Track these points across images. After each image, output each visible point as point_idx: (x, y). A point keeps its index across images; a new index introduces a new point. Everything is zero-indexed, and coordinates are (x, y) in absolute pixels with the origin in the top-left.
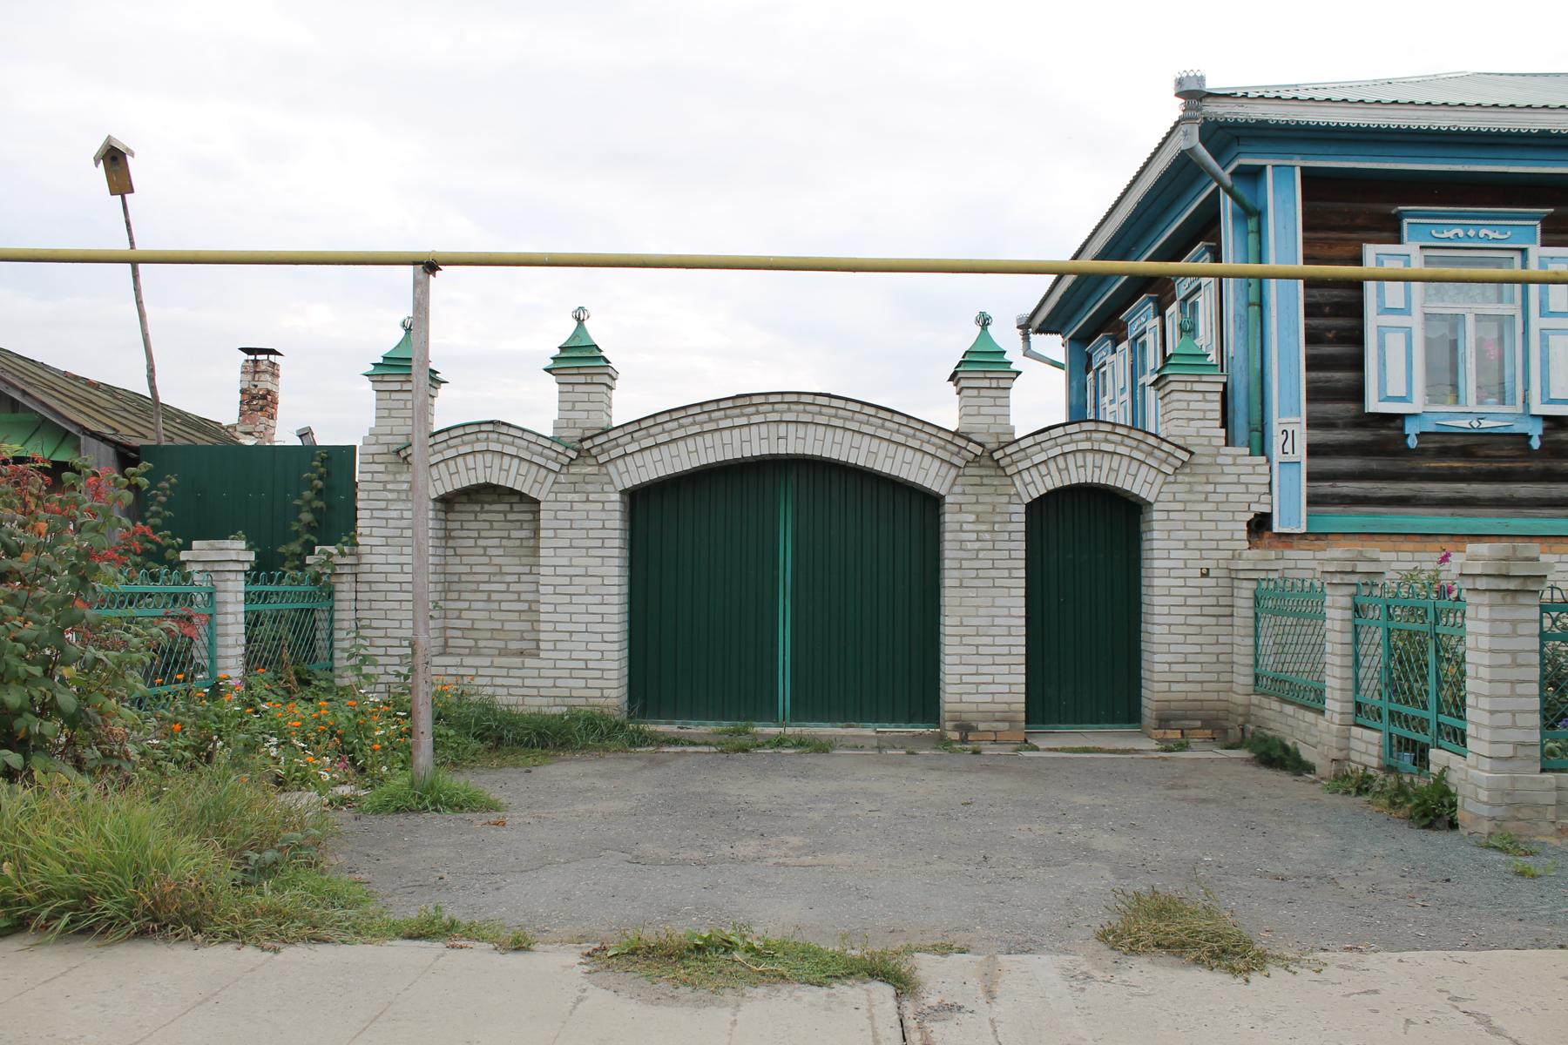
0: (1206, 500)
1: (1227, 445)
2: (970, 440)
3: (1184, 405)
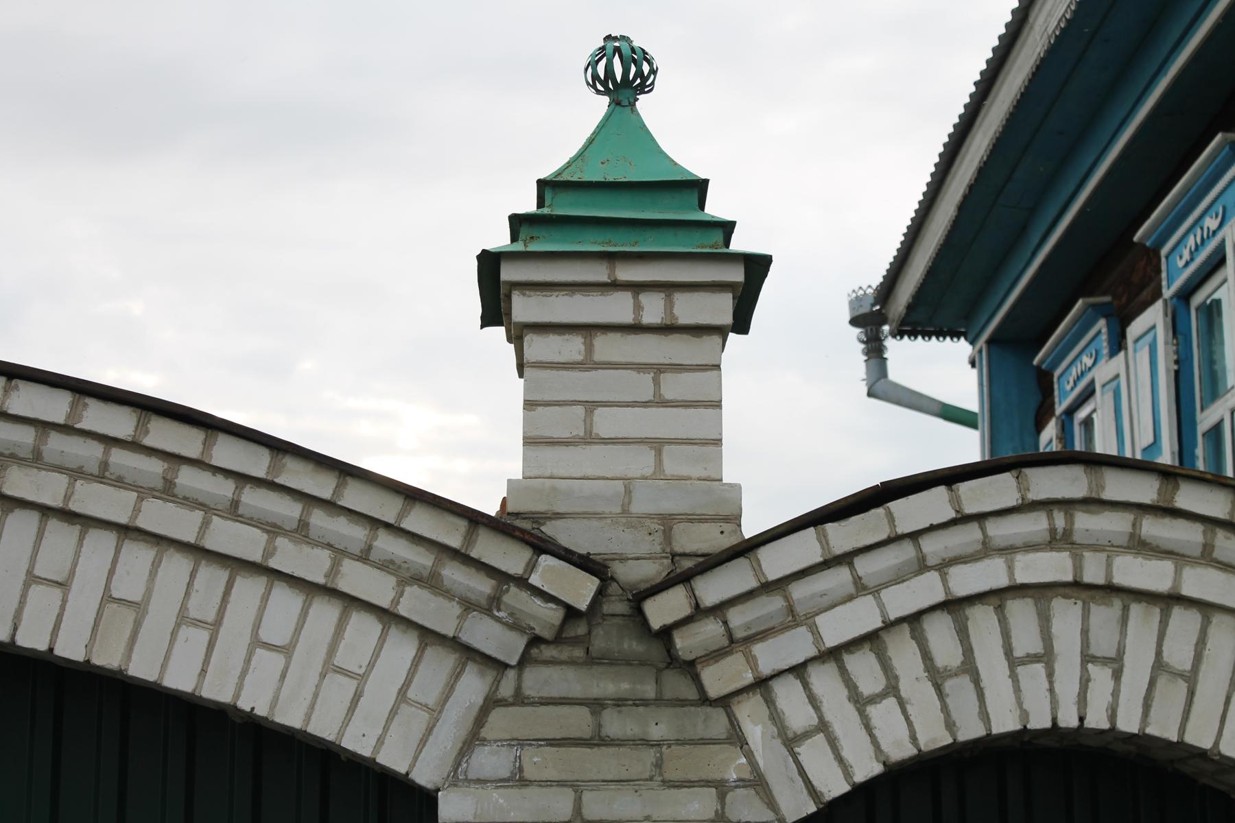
2: (541, 546)
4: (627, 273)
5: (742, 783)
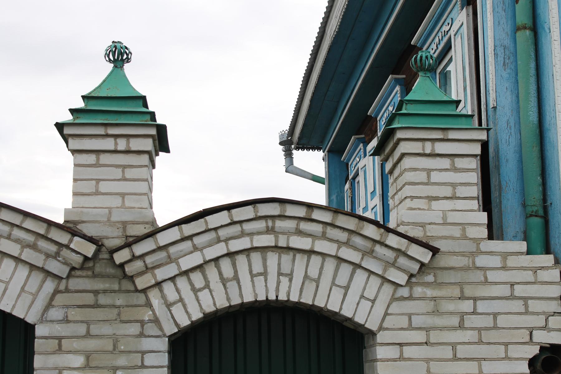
0: (461, 326)
1: (491, 237)
2: (74, 233)
3: (422, 176)
4: (112, 131)
5: (150, 321)
